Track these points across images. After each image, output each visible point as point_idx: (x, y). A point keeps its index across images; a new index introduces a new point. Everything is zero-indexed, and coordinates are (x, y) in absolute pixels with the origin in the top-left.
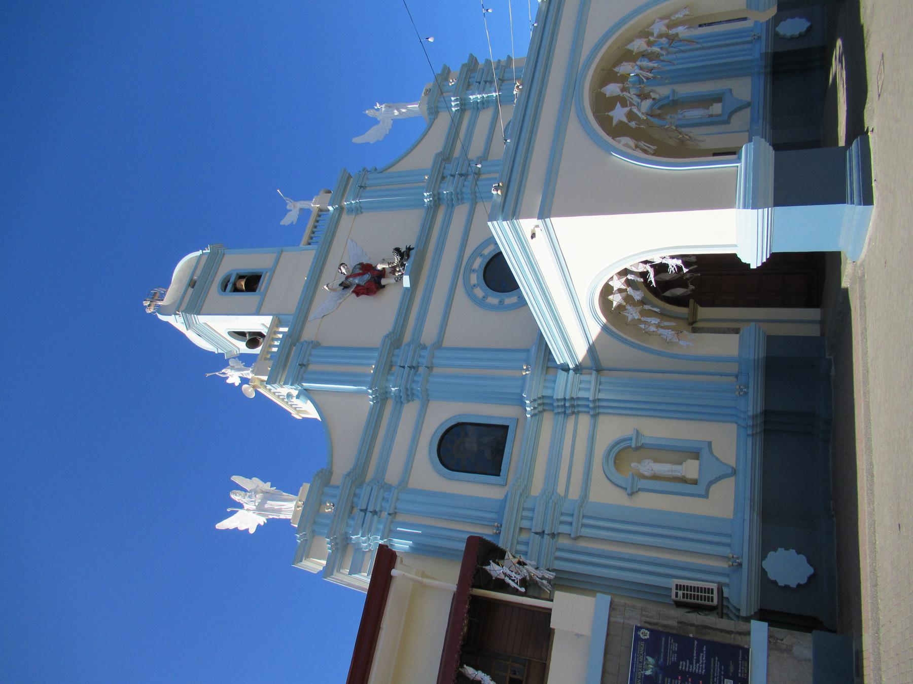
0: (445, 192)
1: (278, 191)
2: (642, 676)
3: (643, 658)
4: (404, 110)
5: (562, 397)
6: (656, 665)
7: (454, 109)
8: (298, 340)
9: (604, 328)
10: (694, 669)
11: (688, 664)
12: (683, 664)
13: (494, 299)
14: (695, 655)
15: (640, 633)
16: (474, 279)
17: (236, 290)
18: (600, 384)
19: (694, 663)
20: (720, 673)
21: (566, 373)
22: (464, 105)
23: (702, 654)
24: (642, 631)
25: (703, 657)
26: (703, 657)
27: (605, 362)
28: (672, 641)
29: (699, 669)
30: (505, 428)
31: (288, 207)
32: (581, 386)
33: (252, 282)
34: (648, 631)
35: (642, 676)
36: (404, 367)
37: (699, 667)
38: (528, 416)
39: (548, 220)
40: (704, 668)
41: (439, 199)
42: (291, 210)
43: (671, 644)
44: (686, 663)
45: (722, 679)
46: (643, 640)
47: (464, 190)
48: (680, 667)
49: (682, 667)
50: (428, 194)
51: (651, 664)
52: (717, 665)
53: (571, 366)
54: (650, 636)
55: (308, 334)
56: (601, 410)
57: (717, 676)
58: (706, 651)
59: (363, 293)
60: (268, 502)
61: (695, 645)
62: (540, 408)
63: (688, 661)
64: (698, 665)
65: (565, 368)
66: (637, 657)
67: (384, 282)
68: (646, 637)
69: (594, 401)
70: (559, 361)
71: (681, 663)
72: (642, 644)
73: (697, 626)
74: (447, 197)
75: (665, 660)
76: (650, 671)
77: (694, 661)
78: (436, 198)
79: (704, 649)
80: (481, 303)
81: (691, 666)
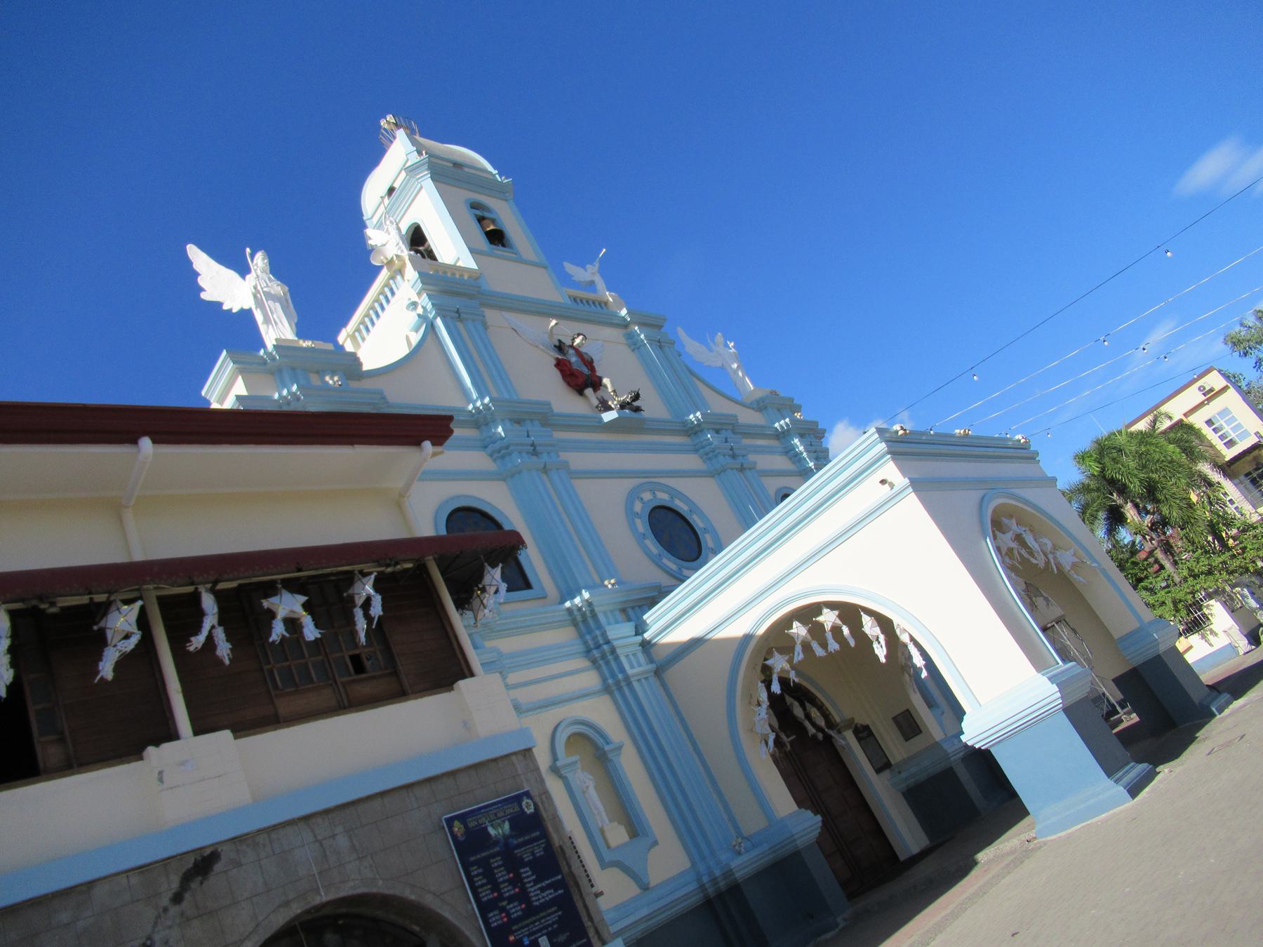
0: (709, 436)
1: (604, 250)
2: (483, 824)
3: (503, 817)
4: (740, 374)
5: (610, 638)
6: (506, 838)
7: (777, 425)
8: (483, 305)
9: (748, 638)
13: (642, 526)
14: (547, 882)
16: (647, 496)
17: (481, 220)
18: (646, 678)
21: (634, 633)
22: (783, 436)
23: (552, 891)
24: (529, 801)
25: (549, 895)
26: (551, 894)
27: (672, 674)
29: (535, 896)
30: (528, 586)
31: (588, 266)
32: (632, 657)
33: (497, 237)
34: (535, 809)
36: (528, 436)
37: (538, 895)
38: (568, 604)
39: (910, 489)
41: (696, 433)
42: (586, 270)
46: (521, 806)
47: (721, 457)
50: (700, 417)
51: (502, 830)
53: (647, 635)
55: (492, 315)
56: (617, 694)
58: (559, 895)
59: (562, 372)
60: (278, 305)
62: (579, 618)
63: (534, 877)
64: (539, 892)
65: (640, 628)
66: (499, 808)
67: (589, 392)
68: (526, 810)
69: (627, 679)
70: (649, 617)
72: (517, 809)
74: (704, 440)
75: (519, 846)
78: (697, 429)
80: (631, 514)
81: (532, 884)
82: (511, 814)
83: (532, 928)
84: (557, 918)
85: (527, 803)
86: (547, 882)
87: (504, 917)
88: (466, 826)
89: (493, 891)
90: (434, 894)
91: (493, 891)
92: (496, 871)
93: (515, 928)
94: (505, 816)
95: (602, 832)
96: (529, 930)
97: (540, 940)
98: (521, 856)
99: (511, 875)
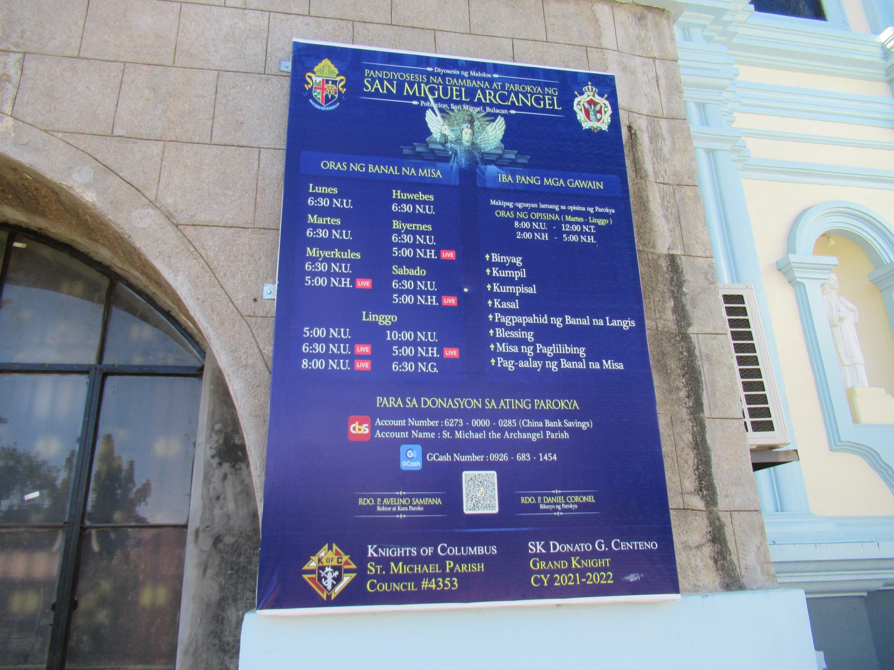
2: (414, 97)
3: (491, 105)
10: (507, 320)
11: (519, 290)
12: (513, 267)
14: (570, 321)
15: (589, 93)
19: (531, 320)
20: (526, 446)
23: (581, 352)
24: (602, 102)
28: (602, 222)
34: (610, 127)
35: (414, 97)
37: (523, 342)
40: (522, 364)
43: (585, 215)
44: (521, 282)
45: (494, 457)
48: (496, 258)
49: (502, 266)
52: (554, 430)
54: (589, 131)
57: (502, 430)
58: (603, 372)
61: (615, 323)
64: (530, 336)
66: (491, 81)
68: (581, 116)
71: (518, 261)
72: (550, 99)
73: (685, 337)
76: (447, 131)
77: (543, 320)
79: (608, 365)
81: (514, 305)
82: (525, 107)
83: (452, 430)
84: (565, 435)
85: (591, 102)
86: (570, 321)
87: (363, 357)
88: (354, 85)
89: (358, 270)
90: (169, 217)
91: (358, 270)
92: (396, 224)
93: (382, 401)
94: (499, 107)
95: (850, 395)
96: (438, 430)
97: (466, 475)
98: (511, 221)
99: (449, 255)
